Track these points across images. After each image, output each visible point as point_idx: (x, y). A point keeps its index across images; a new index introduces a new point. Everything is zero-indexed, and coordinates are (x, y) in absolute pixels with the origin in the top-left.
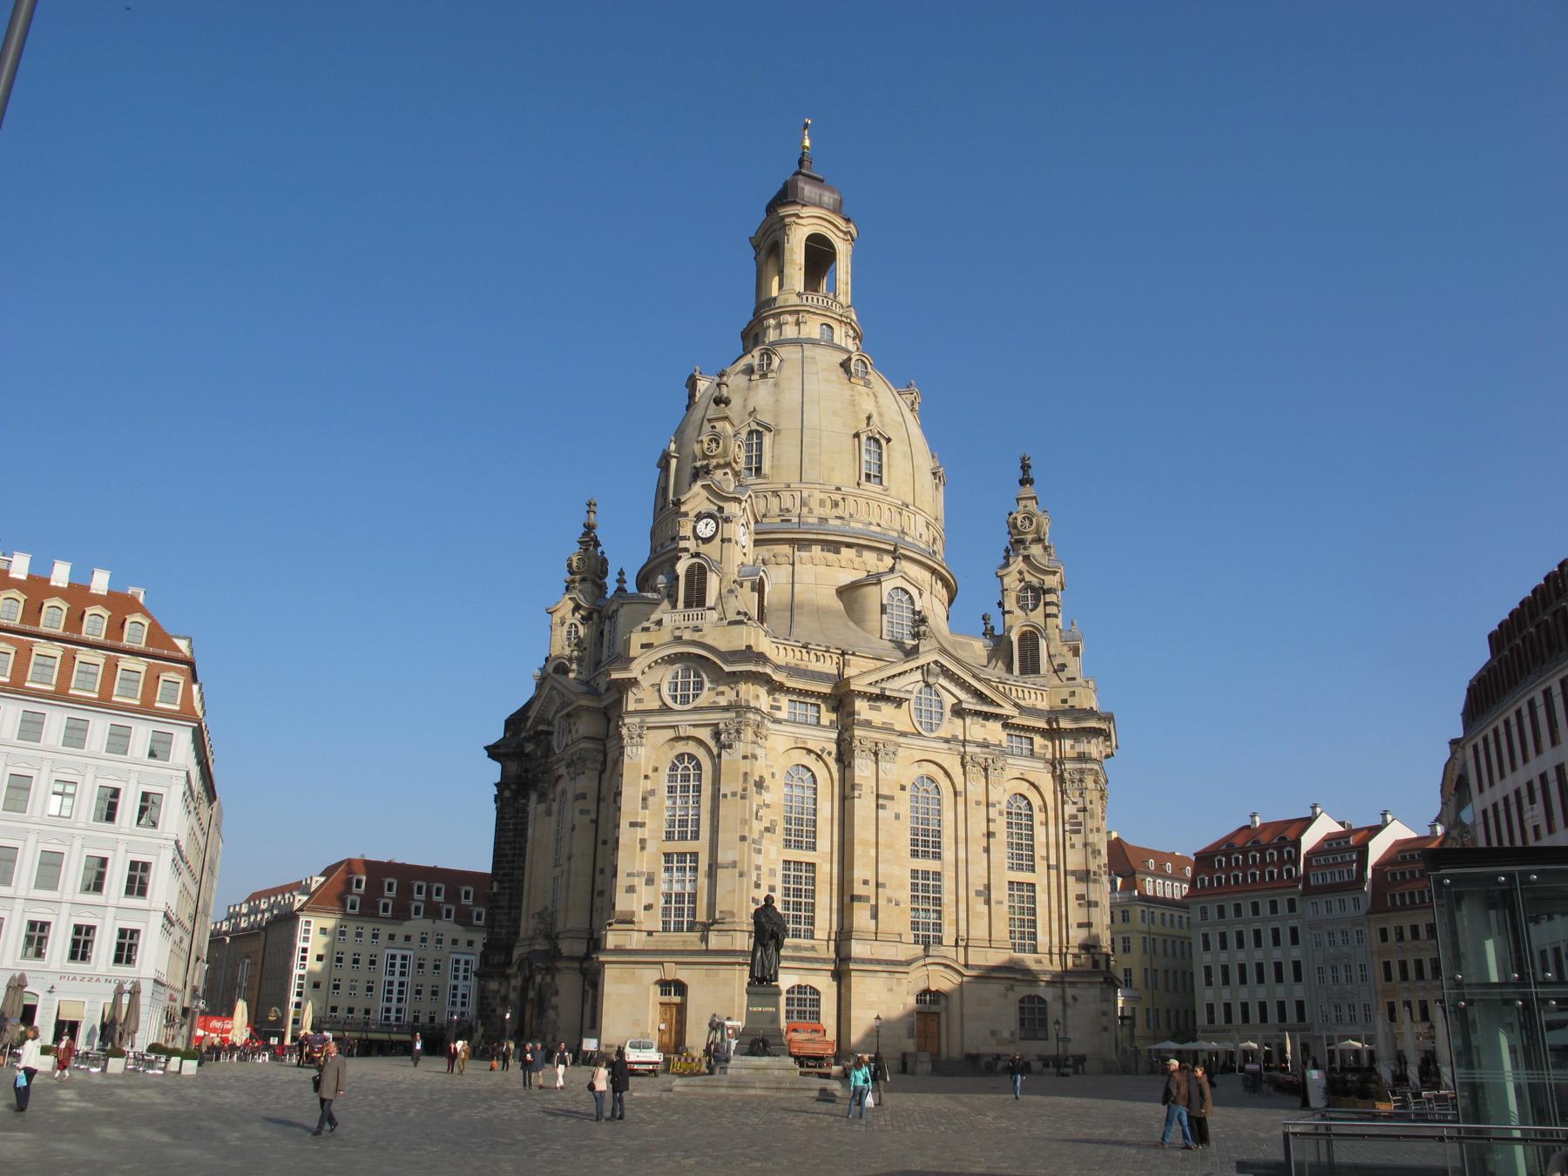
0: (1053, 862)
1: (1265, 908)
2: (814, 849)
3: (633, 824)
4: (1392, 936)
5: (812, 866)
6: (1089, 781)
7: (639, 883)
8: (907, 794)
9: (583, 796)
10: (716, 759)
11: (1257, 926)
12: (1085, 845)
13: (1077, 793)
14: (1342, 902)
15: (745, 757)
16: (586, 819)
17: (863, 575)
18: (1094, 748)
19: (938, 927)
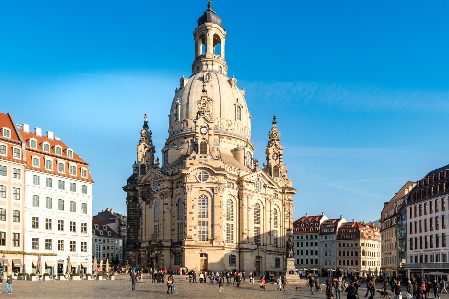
0: (281, 226)
3: (190, 213)
7: (192, 228)
9: (167, 204)
11: (307, 241)
14: (330, 237)
15: (220, 197)
16: (169, 210)
18: (291, 197)
19: (259, 240)
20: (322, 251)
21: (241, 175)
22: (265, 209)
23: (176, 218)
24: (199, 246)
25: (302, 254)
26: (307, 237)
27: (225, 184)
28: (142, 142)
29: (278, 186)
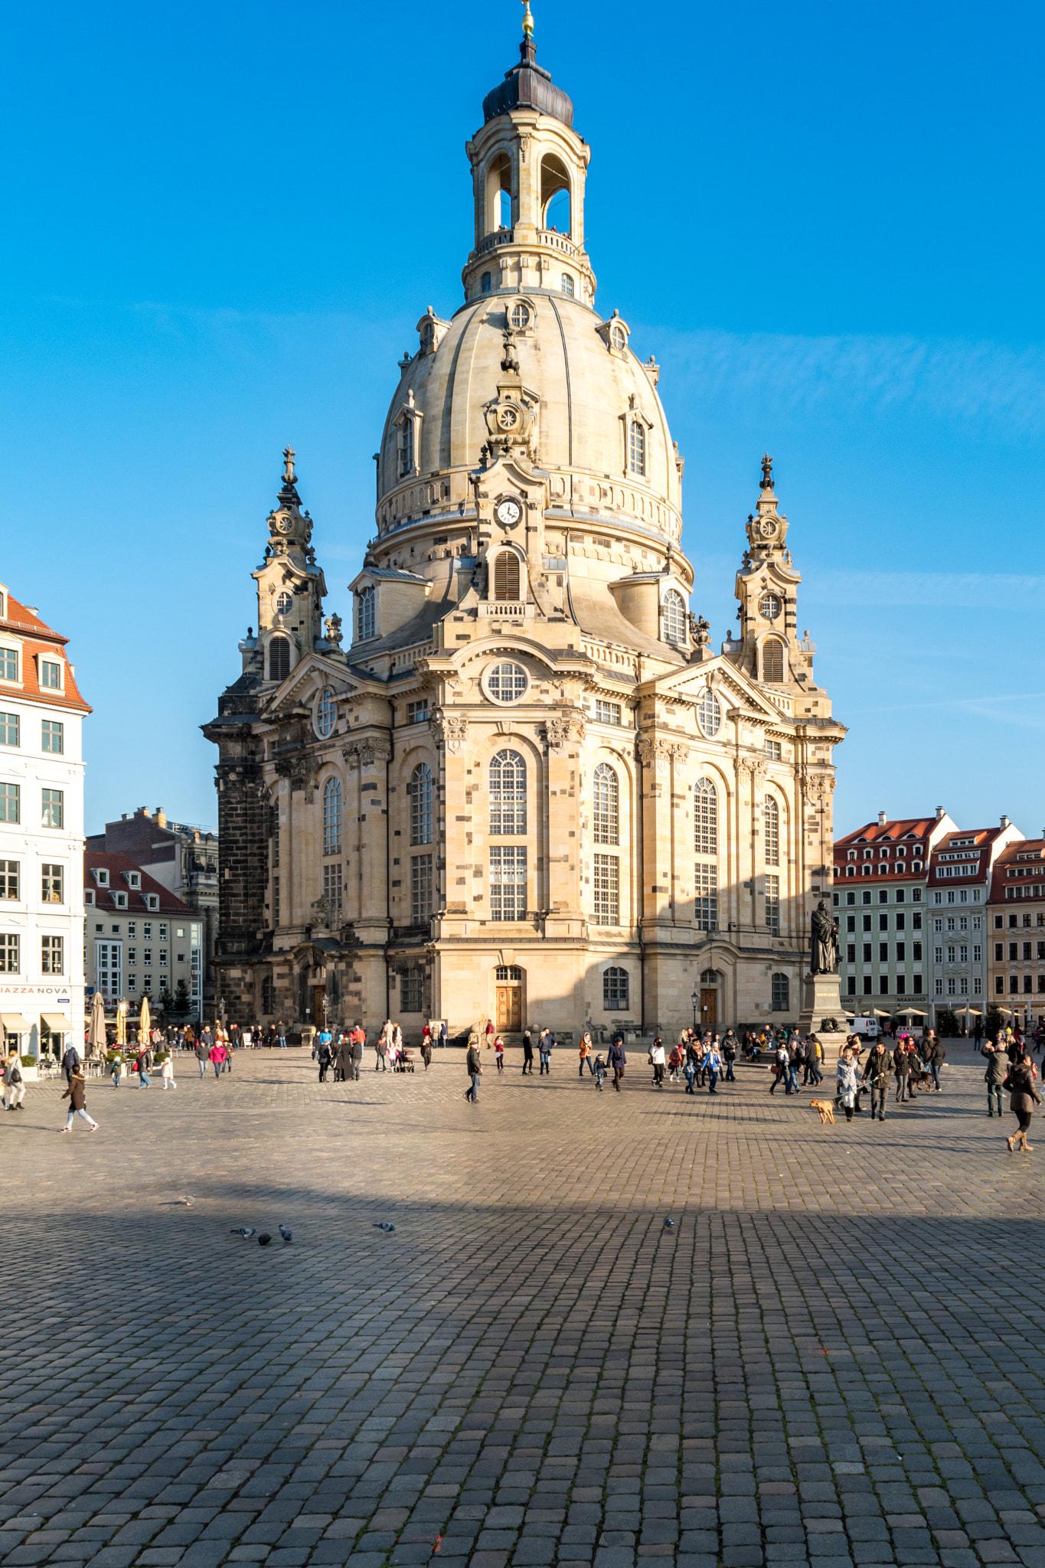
0: (793, 857)
1: (875, 898)
2: (617, 843)
3: (460, 819)
4: (1006, 922)
5: (616, 859)
6: (827, 783)
8: (693, 793)
9: (374, 786)
10: (543, 759)
11: (884, 912)
12: (822, 843)
13: (816, 796)
15: (571, 756)
17: (628, 572)
18: (828, 754)
19: (714, 914)
20: (939, 944)
21: (646, 676)
22: (733, 800)
23: (406, 837)
24: (494, 940)
25: (868, 958)
26: (883, 896)
27: (588, 708)
28: (276, 556)
29: (780, 714)
